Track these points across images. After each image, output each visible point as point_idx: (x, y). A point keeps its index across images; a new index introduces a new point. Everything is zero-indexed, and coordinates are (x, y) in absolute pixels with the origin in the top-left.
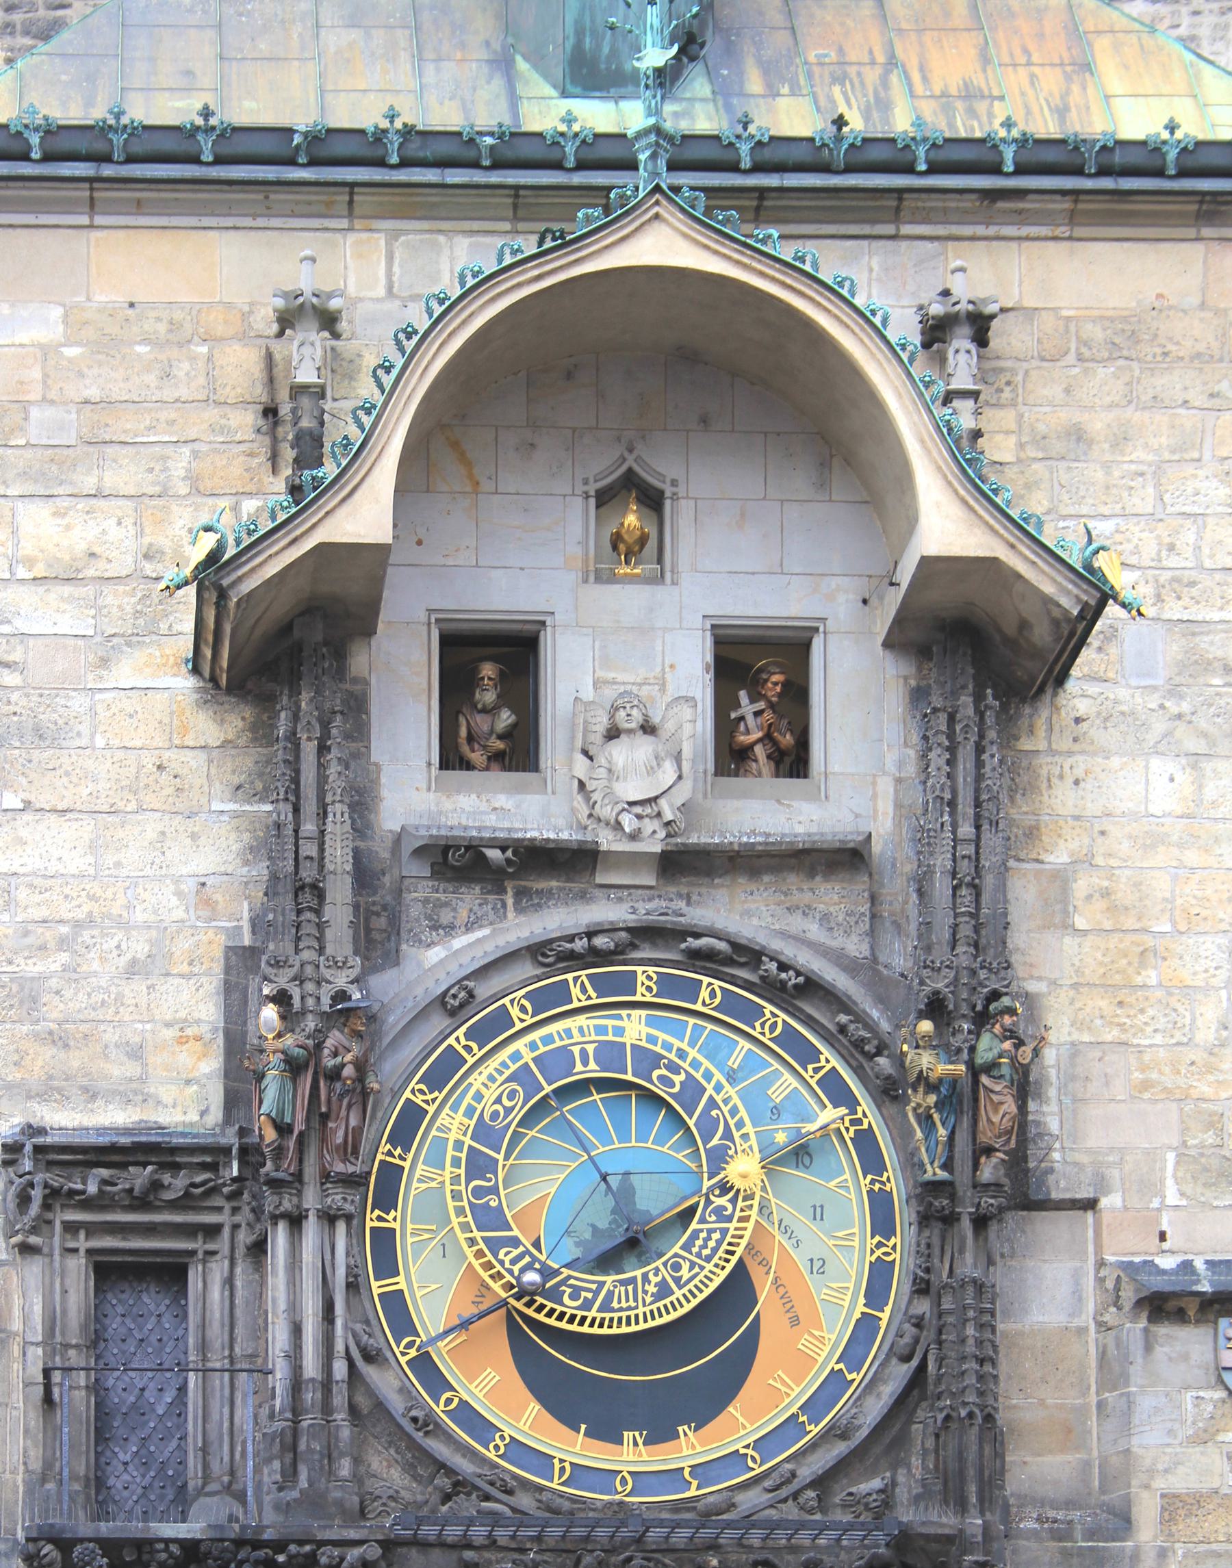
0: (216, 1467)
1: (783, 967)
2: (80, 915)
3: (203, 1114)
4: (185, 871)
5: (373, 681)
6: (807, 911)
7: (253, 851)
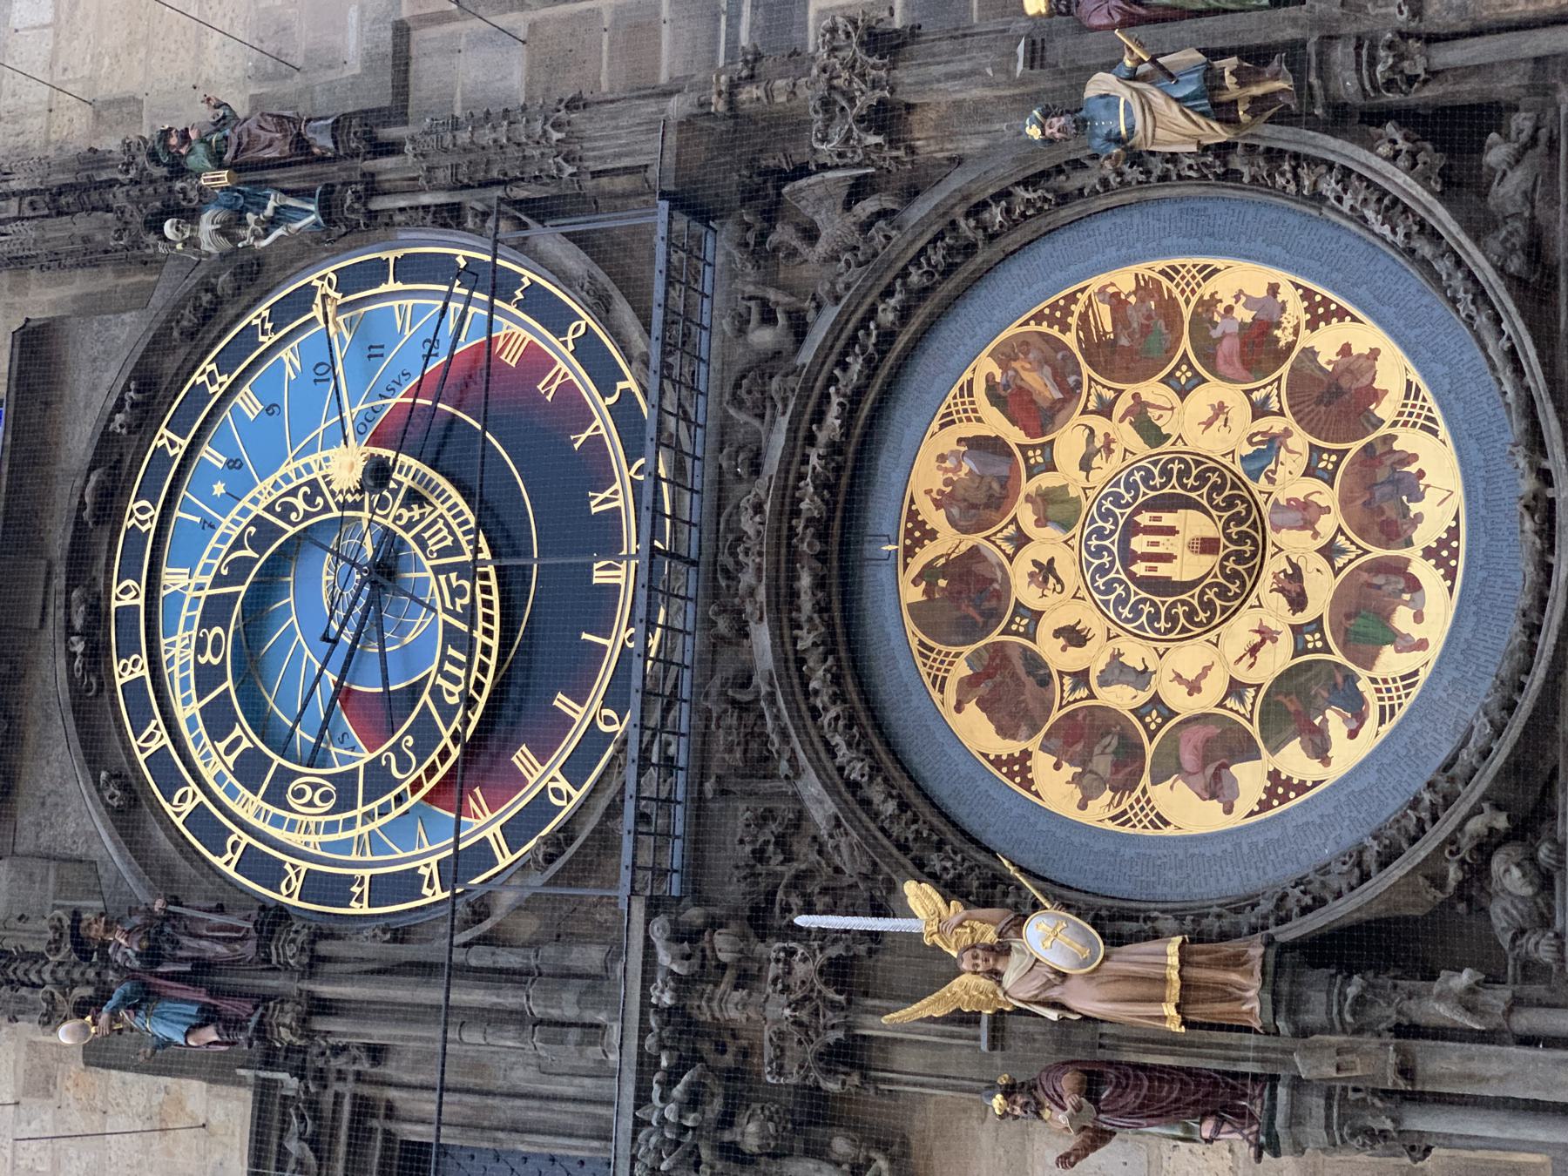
1: (119, 407)
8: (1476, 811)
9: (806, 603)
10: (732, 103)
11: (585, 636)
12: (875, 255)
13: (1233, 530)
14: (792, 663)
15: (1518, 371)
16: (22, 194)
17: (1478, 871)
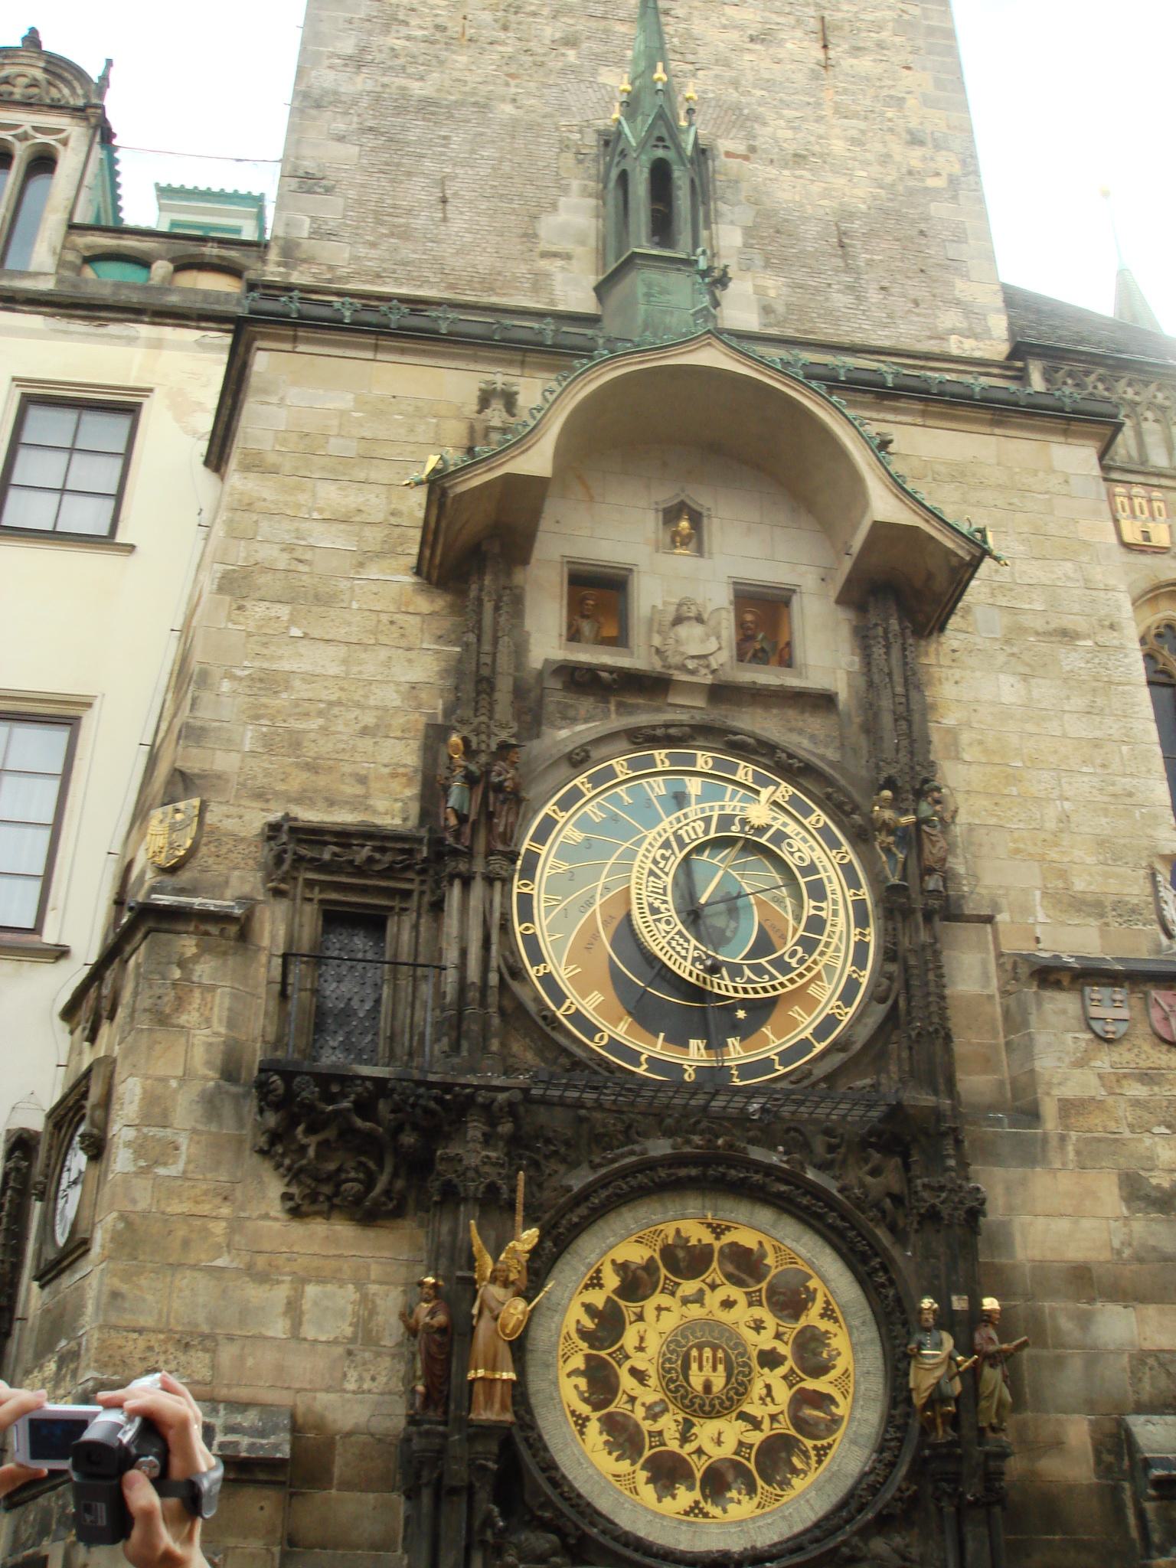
0: (398, 1051)
1: (791, 756)
2: (333, 698)
3: (405, 820)
4: (403, 679)
5: (527, 588)
6: (801, 732)
7: (445, 673)
8: (577, 1528)
9: (683, 1172)
10: (943, 1135)
11: (662, 1035)
12: (863, 1212)
13: (717, 1402)
14: (650, 1165)
15: (792, 1551)
16: (907, 696)
17: (545, 1526)
